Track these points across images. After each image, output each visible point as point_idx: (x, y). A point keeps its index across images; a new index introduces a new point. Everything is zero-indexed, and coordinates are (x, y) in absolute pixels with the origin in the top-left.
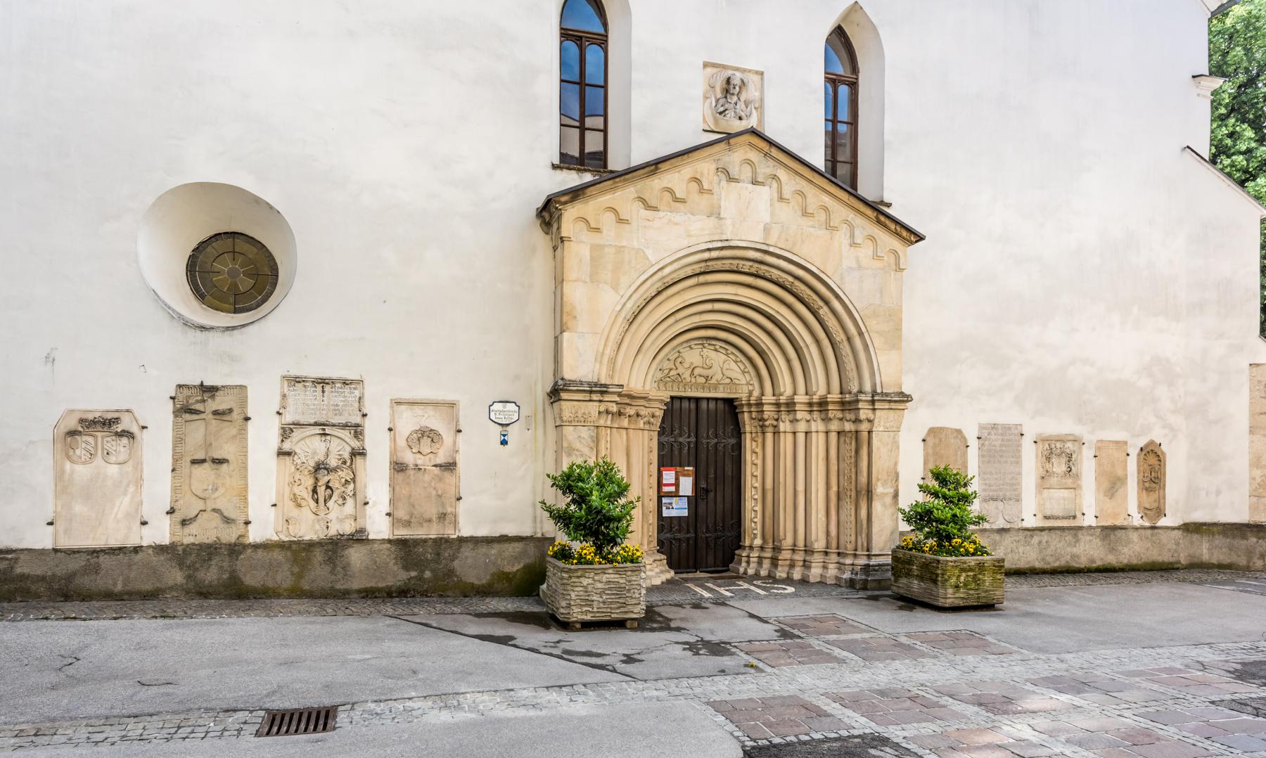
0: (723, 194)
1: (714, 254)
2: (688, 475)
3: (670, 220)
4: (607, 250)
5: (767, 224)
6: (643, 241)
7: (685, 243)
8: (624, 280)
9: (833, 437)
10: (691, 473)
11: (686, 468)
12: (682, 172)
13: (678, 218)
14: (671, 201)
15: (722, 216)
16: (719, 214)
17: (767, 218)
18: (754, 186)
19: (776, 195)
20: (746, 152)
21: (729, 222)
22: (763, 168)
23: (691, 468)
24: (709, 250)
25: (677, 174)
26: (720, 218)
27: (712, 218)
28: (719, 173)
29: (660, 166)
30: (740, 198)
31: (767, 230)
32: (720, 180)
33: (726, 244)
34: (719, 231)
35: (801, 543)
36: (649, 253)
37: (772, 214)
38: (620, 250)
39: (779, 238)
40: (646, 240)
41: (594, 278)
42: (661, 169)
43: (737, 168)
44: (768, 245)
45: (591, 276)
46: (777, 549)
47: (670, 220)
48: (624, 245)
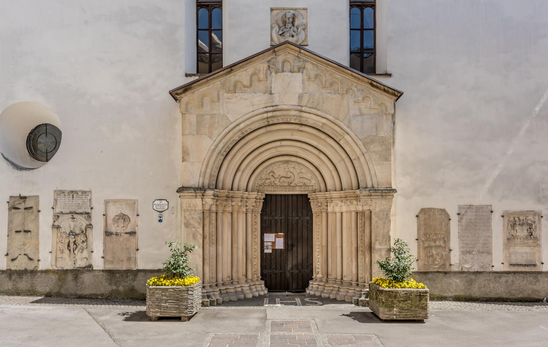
0: (273, 79)
1: (270, 114)
2: (281, 237)
3: (241, 97)
4: (206, 117)
5: (301, 94)
6: (226, 110)
7: (251, 109)
8: (216, 133)
9: (353, 214)
10: (282, 236)
11: (279, 234)
12: (248, 70)
13: (246, 96)
14: (242, 86)
15: (272, 92)
16: (271, 91)
17: (300, 91)
18: (292, 73)
19: (306, 77)
20: (286, 55)
21: (276, 96)
22: (297, 63)
23: (282, 234)
24: (267, 112)
25: (245, 72)
26: (271, 94)
27: (267, 94)
28: (270, 69)
29: (233, 68)
30: (284, 81)
31: (300, 97)
32: (271, 72)
33: (275, 108)
34: (271, 101)
35: (339, 277)
36: (230, 116)
37: (304, 88)
38: (213, 116)
39: (308, 101)
40: (227, 109)
41: (198, 132)
42: (234, 70)
43: (281, 65)
44: (301, 106)
45: (197, 131)
46: (327, 281)
47: (241, 97)
48: (215, 113)
